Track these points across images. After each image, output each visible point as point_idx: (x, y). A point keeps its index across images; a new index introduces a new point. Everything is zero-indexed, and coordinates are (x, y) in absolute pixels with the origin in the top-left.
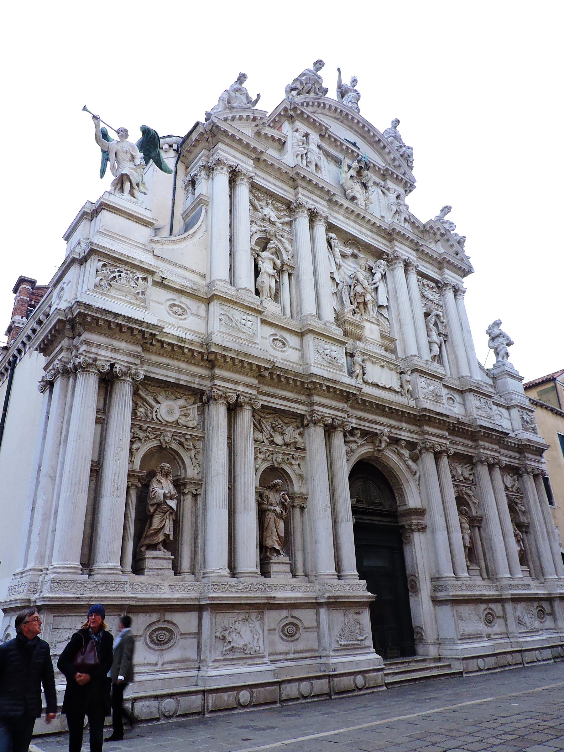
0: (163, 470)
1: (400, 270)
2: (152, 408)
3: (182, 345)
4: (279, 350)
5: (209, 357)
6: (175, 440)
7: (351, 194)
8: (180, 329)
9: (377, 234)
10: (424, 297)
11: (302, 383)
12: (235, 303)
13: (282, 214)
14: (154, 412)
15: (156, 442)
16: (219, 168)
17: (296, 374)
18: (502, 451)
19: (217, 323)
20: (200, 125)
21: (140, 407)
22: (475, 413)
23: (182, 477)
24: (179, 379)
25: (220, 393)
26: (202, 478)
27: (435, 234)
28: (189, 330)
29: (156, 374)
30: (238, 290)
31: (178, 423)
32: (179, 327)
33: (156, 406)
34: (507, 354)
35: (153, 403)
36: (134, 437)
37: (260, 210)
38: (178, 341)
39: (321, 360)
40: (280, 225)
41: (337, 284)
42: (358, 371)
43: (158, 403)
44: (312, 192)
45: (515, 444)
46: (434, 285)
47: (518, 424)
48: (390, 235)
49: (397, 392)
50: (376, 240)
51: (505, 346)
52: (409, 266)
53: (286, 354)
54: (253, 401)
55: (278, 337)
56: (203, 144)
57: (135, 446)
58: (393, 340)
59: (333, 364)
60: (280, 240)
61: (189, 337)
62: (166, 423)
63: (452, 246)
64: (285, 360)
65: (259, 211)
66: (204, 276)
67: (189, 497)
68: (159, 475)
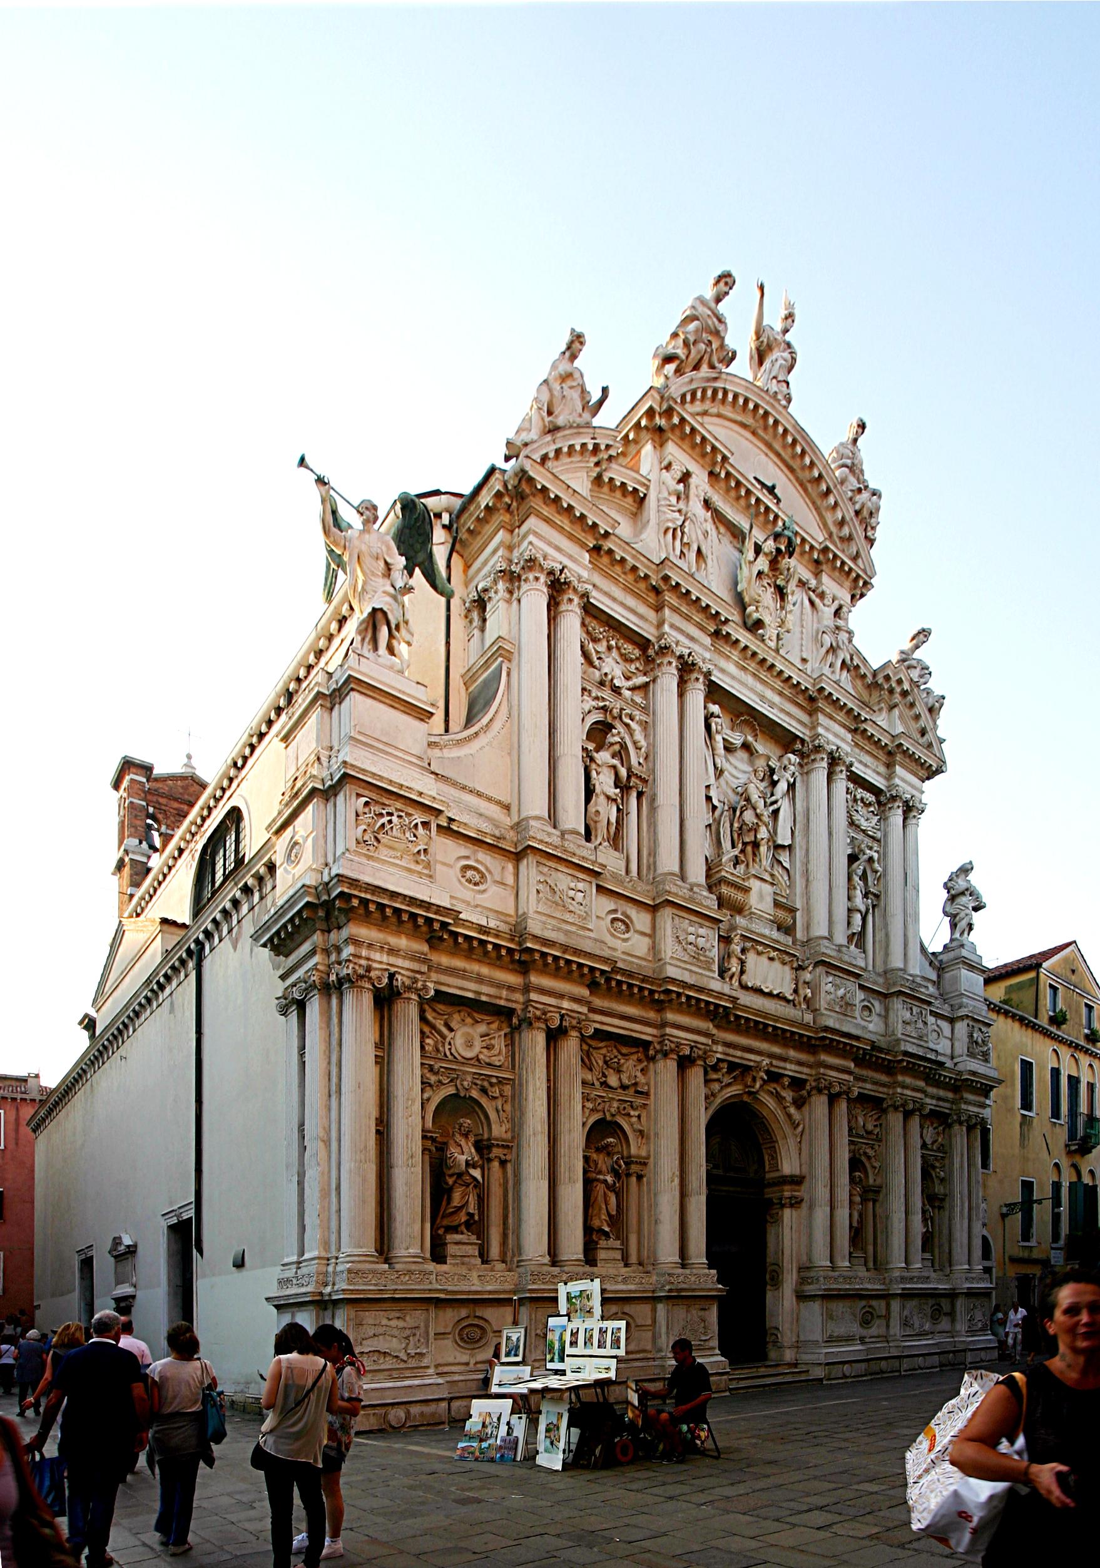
5: (522, 955)
8: (479, 909)
13: (633, 667)
16: (531, 576)
20: (497, 475)
28: (490, 910)
29: (448, 985)
30: (563, 834)
32: (477, 906)
37: (597, 662)
38: (479, 933)
39: (679, 952)
42: (734, 969)
56: (502, 517)
57: (426, 1096)
59: (698, 959)
61: (492, 924)
65: (595, 667)
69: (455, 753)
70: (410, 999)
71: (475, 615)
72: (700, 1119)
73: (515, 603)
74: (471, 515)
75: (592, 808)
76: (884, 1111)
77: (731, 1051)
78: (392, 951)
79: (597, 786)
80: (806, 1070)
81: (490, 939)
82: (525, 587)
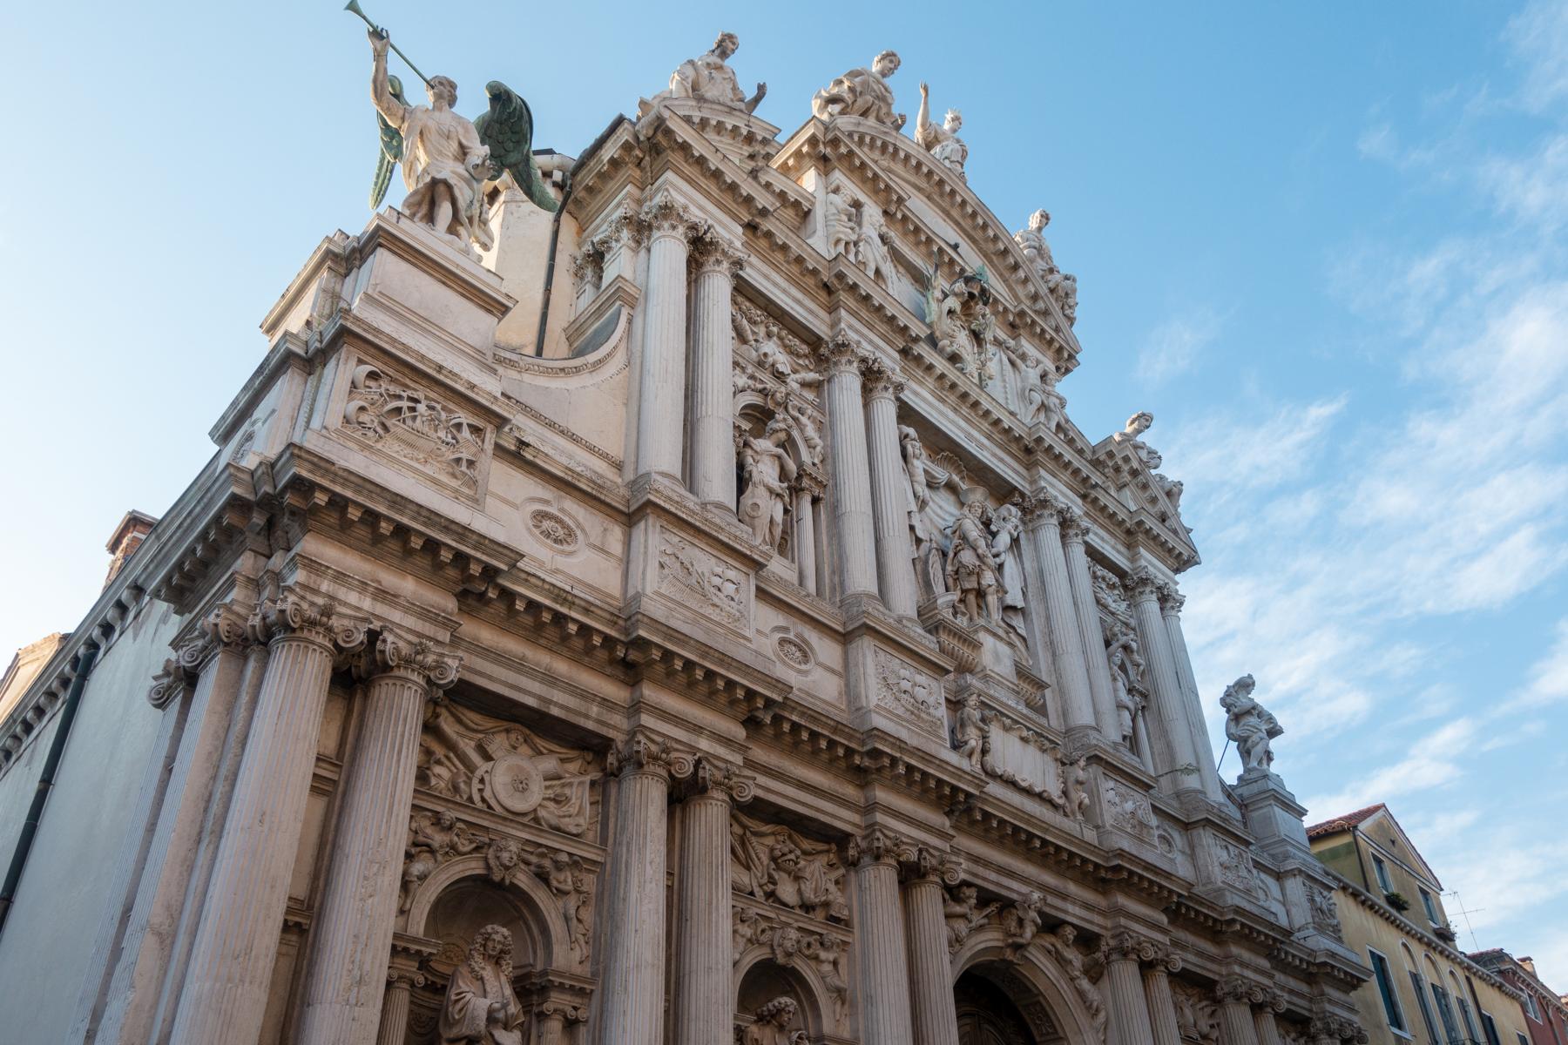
0: (490, 944)
1: (1050, 533)
2: (471, 768)
3: (564, 610)
4: (792, 668)
5: (630, 653)
6: (528, 863)
7: (949, 349)
9: (1000, 446)
10: (1098, 601)
11: (850, 752)
12: (698, 531)
14: (475, 782)
15: (473, 864)
17: (838, 727)
18: (1280, 977)
19: (652, 572)
21: (439, 762)
22: (1218, 876)
23: (539, 967)
24: (550, 702)
25: (654, 748)
26: (595, 974)
27: (1117, 470)
31: (536, 820)
33: (483, 767)
34: (1269, 756)
35: (475, 758)
36: (415, 844)
38: (555, 600)
40: (795, 386)
41: (919, 541)
42: (973, 743)
43: (488, 757)
44: (871, 327)
45: (1301, 960)
46: (1115, 579)
47: (1301, 916)
48: (1028, 451)
49: (1055, 806)
50: (1001, 460)
51: (1264, 735)
52: (1070, 527)
53: (810, 678)
54: (735, 779)
55: (791, 636)
58: (1041, 686)
60: (795, 419)
62: (505, 814)
63: (1154, 500)
64: (808, 694)
66: (619, 466)
67: (555, 1026)
68: (478, 958)
69: (542, 381)
70: (407, 680)
71: (589, 272)
72: (942, 975)
73: (643, 253)
74: (590, 171)
75: (747, 499)
76: (1218, 1002)
77: (980, 870)
78: (382, 595)
79: (755, 474)
80: (1097, 919)
81: (574, 615)
82: (656, 234)
